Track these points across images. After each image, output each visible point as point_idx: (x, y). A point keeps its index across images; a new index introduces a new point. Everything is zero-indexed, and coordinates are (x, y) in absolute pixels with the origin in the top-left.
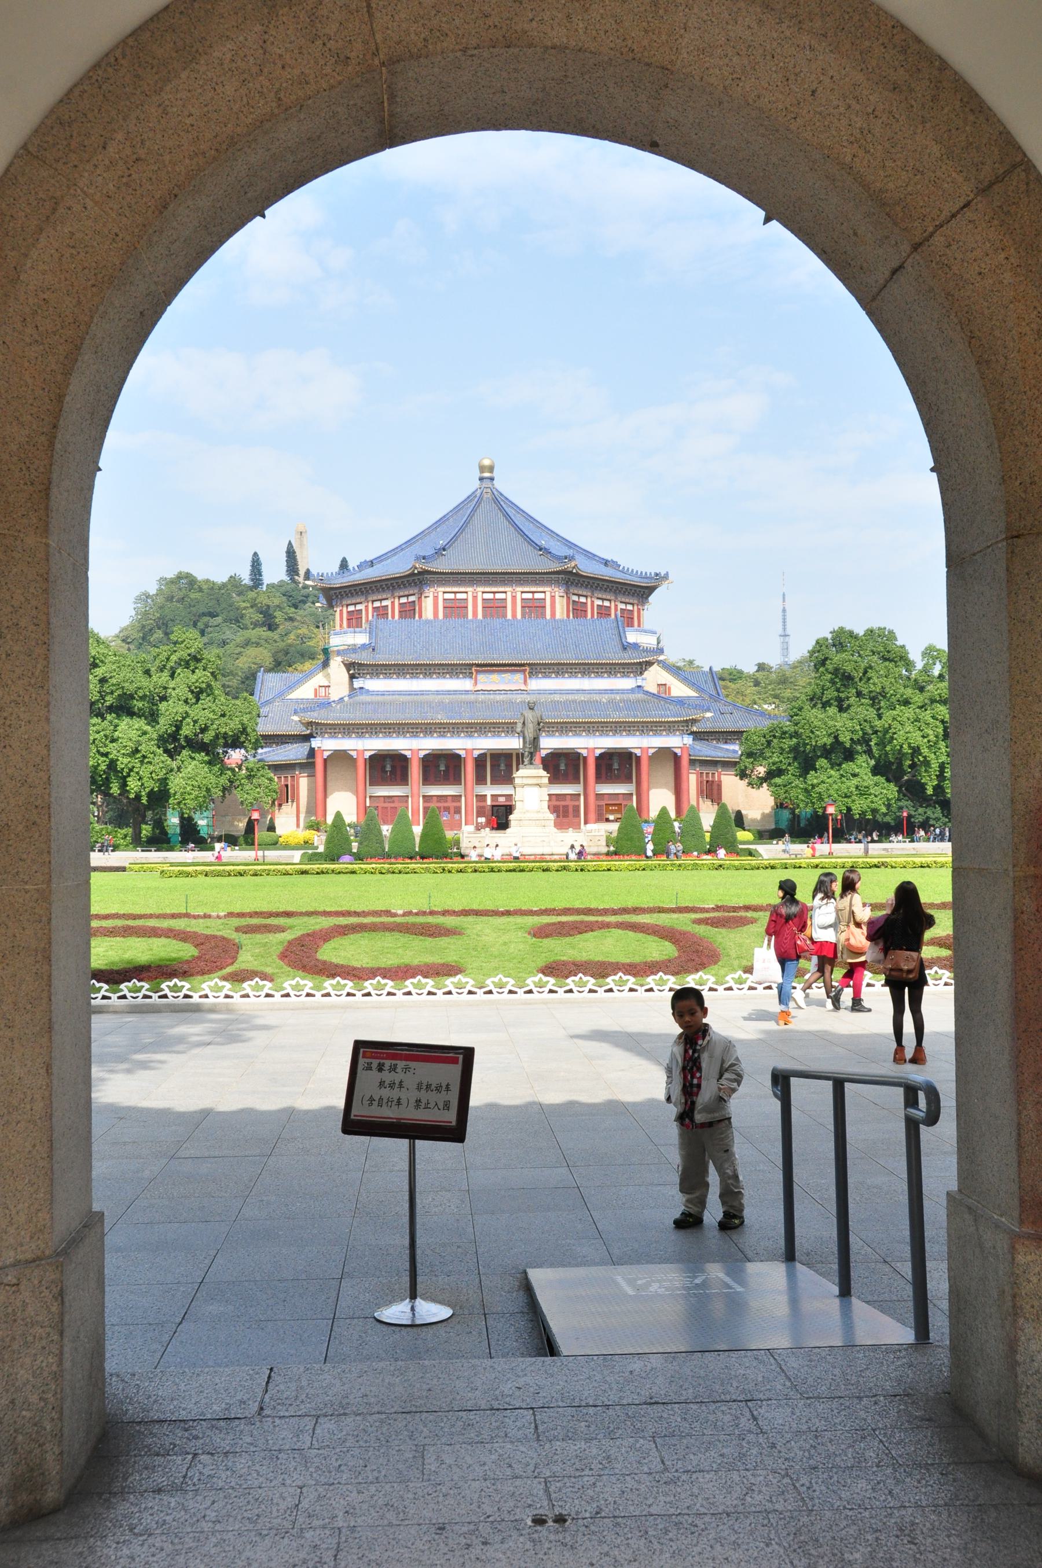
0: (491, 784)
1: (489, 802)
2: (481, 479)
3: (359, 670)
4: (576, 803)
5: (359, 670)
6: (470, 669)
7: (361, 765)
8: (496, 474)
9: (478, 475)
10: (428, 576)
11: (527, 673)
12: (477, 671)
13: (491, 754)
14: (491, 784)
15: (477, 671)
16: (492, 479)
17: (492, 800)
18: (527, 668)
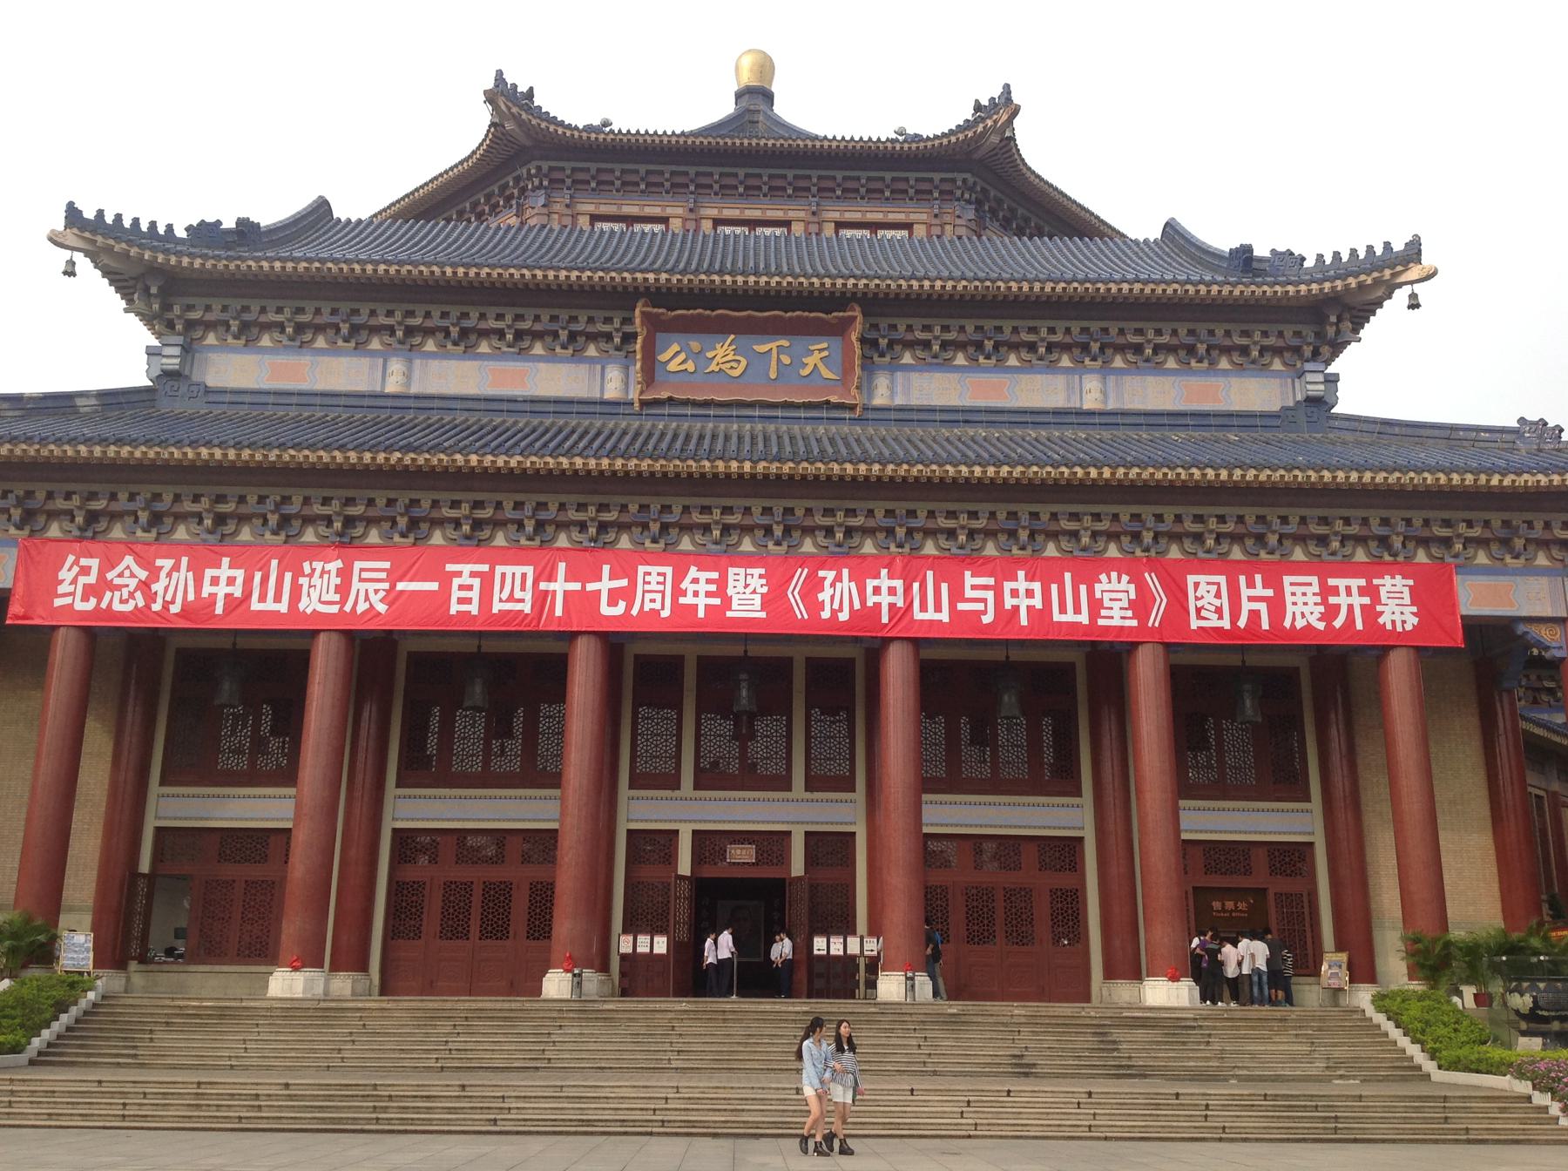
0: (697, 787)
1: (684, 866)
2: (739, 96)
3: (167, 307)
4: (1064, 880)
5: (167, 307)
6: (628, 321)
7: (64, 656)
8: (775, 88)
9: (736, 88)
10: (545, 165)
11: (854, 337)
12: (656, 326)
13: (704, 663)
14: (697, 787)
15: (650, 320)
16: (768, 97)
17: (697, 859)
18: (857, 313)
